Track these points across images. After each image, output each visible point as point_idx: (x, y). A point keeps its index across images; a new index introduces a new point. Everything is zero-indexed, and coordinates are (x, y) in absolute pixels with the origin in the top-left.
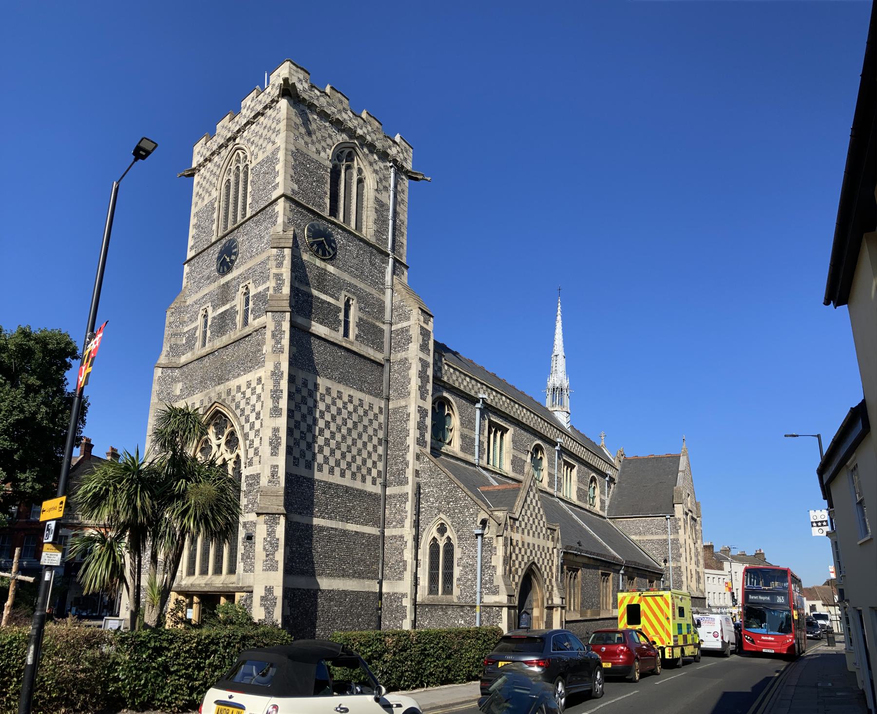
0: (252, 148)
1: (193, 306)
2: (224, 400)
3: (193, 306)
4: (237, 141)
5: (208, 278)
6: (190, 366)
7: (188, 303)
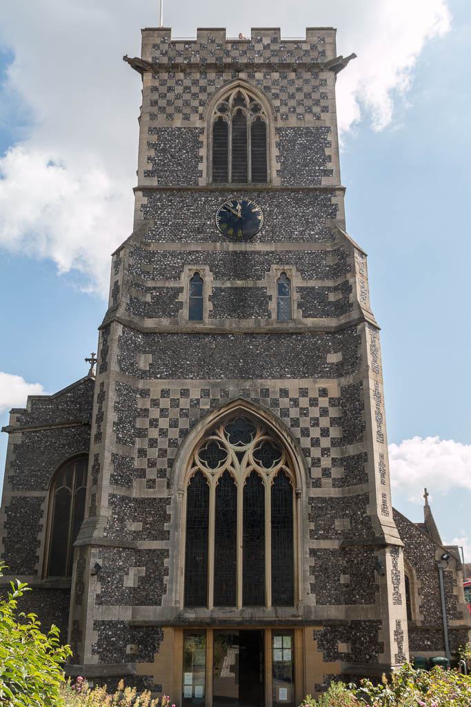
0: (277, 103)
2: (256, 400)
3: (164, 256)
4: (242, 75)
5: (199, 231)
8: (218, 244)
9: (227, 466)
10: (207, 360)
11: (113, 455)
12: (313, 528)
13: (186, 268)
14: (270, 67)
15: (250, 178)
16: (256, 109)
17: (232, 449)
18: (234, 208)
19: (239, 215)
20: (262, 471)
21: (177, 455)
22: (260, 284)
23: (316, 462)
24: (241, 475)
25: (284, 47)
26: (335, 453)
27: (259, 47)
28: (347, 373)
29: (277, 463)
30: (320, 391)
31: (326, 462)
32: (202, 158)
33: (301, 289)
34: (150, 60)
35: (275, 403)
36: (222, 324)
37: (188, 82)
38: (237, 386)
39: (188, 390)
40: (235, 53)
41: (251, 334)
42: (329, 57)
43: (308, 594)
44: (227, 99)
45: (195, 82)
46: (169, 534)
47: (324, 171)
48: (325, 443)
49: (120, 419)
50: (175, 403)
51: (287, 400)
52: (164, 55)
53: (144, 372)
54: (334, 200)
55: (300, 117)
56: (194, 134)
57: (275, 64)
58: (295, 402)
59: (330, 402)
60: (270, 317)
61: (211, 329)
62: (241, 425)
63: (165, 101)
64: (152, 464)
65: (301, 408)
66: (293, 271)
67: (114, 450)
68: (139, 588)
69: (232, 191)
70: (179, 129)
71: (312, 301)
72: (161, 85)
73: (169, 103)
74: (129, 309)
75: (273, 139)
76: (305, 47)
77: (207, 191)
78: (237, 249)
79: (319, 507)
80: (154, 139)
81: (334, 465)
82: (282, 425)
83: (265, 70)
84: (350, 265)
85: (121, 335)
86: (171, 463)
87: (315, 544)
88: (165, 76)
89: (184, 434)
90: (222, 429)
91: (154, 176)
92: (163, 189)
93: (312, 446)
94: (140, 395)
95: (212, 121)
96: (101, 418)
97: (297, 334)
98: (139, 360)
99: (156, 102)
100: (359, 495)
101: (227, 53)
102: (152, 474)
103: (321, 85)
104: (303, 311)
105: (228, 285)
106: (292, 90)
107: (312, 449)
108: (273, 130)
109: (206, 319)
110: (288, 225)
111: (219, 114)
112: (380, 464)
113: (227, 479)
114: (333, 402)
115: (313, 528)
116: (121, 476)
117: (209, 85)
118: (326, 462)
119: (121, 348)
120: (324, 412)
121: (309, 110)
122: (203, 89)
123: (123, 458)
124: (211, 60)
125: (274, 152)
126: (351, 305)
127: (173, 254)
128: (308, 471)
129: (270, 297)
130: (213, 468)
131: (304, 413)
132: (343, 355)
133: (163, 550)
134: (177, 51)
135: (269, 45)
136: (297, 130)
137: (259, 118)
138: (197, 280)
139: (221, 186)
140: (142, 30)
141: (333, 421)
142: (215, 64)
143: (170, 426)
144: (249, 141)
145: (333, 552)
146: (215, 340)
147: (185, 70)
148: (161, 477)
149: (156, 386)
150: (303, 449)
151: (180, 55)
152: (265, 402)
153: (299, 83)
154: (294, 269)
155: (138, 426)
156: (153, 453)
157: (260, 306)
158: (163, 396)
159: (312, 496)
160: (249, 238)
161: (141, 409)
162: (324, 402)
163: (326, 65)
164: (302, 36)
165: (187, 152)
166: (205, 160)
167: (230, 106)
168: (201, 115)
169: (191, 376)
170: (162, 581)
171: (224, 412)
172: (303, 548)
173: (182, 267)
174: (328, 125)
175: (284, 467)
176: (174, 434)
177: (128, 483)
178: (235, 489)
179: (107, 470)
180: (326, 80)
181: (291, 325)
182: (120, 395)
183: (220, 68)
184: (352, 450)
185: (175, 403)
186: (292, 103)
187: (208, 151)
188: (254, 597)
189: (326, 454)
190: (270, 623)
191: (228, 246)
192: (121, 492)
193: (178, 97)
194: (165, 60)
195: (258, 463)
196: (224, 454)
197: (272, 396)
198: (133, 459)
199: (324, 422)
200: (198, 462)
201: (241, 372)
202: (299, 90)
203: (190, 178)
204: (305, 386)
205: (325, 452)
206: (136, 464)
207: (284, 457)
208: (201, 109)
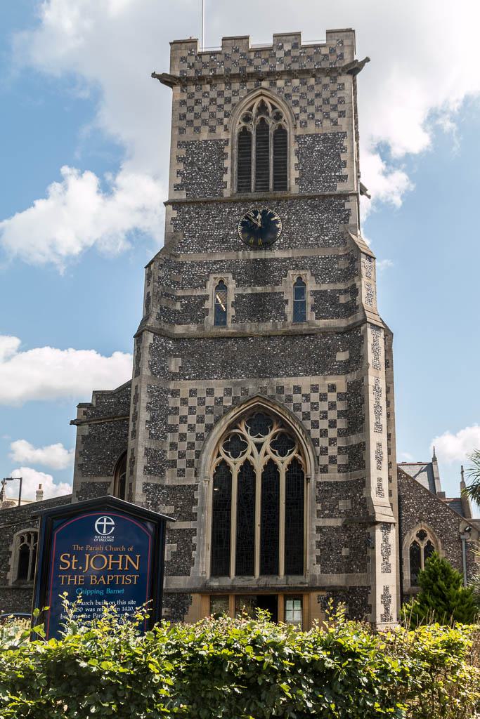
1: (192, 266)
2: (273, 397)
3: (192, 266)
4: (265, 84)
5: (223, 241)
6: (197, 343)
7: (180, 260)
8: (240, 253)
9: (247, 455)
10: (230, 361)
11: (146, 449)
12: (319, 508)
13: (212, 277)
14: (290, 74)
15: (271, 186)
16: (278, 117)
17: (251, 440)
18: (255, 217)
19: (259, 224)
20: (278, 459)
21: (204, 447)
22: (278, 289)
23: (324, 451)
24: (259, 463)
25: (304, 53)
26: (341, 443)
27: (280, 54)
28: (352, 371)
29: (291, 452)
30: (329, 386)
31: (333, 451)
32: (226, 169)
33: (315, 293)
34: (178, 74)
35: (289, 399)
36: (243, 328)
37: (213, 94)
38: (256, 384)
39: (213, 390)
40: (257, 62)
41: (269, 337)
42: (347, 61)
43: (314, 564)
44: (251, 109)
45: (221, 94)
46: (196, 516)
47: (339, 176)
48: (333, 433)
49: (153, 419)
50: (202, 401)
51: (300, 395)
52: (191, 68)
53: (175, 374)
54: (347, 206)
55: (318, 124)
56: (219, 145)
57: (295, 71)
58: (307, 397)
59: (338, 397)
60: (286, 319)
61: (233, 333)
62: (260, 419)
63: (192, 114)
64: (182, 456)
65: (312, 403)
66: (307, 276)
67: (147, 445)
68: (171, 561)
69: (253, 201)
70: (206, 141)
71: (326, 303)
72: (189, 98)
73: (197, 116)
74: (160, 318)
75: (293, 147)
76: (324, 51)
77: (232, 202)
78: (257, 257)
79: (326, 490)
80: (183, 153)
81: (339, 453)
82: (295, 418)
83: (286, 77)
84: (357, 269)
85: (152, 342)
86: (198, 454)
87: (321, 522)
88: (192, 88)
89: (210, 428)
90: (243, 423)
91: (183, 189)
92: (191, 202)
93: (321, 436)
94: (172, 395)
95: (237, 131)
96: (136, 417)
97: (310, 335)
98: (170, 364)
99: (184, 116)
100: (358, 480)
101: (250, 62)
102: (182, 464)
103: (339, 89)
104: (316, 313)
105: (249, 291)
106: (311, 96)
107: (321, 439)
108: (293, 139)
109: (229, 325)
110: (304, 231)
111: (243, 124)
112: (376, 452)
113: (247, 467)
114: (341, 397)
115: (319, 508)
116: (154, 467)
117: (234, 95)
118: (333, 451)
119: (152, 353)
120: (332, 406)
121: (327, 116)
122: (228, 100)
123: (155, 451)
124: (235, 70)
125: (293, 160)
126: (357, 307)
127: (200, 264)
128: (317, 459)
129: (287, 302)
130: (235, 458)
131: (314, 407)
132: (350, 354)
133: (191, 529)
134: (203, 63)
135: (289, 51)
136: (315, 137)
137: (280, 126)
138: (221, 287)
139: (243, 196)
140: (171, 43)
141: (340, 414)
142: (239, 74)
143: (198, 422)
144: (271, 150)
145: (337, 529)
146: (237, 343)
147: (211, 82)
148: (190, 467)
149: (185, 386)
150: (313, 440)
151: (205, 66)
152: (280, 398)
153: (318, 88)
154: (309, 273)
155: (169, 422)
156: (183, 446)
157: (277, 310)
158: (191, 396)
159: (320, 480)
160: (268, 245)
161: (172, 408)
162: (332, 397)
163: (343, 69)
164: (322, 39)
165: (213, 164)
166: (229, 171)
167: (254, 115)
168: (226, 126)
169: (216, 377)
170: (190, 555)
171: (244, 408)
172: (312, 523)
173: (208, 276)
174: (344, 130)
175: (297, 455)
176: (201, 428)
177: (161, 473)
178: (254, 476)
179: (141, 462)
180: (343, 84)
181: (305, 327)
182: (152, 396)
183: (244, 78)
184: (354, 439)
185: (202, 401)
186: (311, 109)
187: (232, 162)
188: (270, 568)
189: (333, 443)
190: (281, 589)
191: (249, 255)
192: (154, 481)
193: (205, 109)
194: (192, 73)
195: (274, 453)
196: (245, 445)
197: (287, 393)
198: (165, 451)
199: (332, 415)
200: (222, 453)
201: (259, 372)
202: (318, 95)
203: (216, 190)
204: (315, 383)
205: (332, 441)
206: (169, 456)
207: (297, 447)
208: (226, 120)
